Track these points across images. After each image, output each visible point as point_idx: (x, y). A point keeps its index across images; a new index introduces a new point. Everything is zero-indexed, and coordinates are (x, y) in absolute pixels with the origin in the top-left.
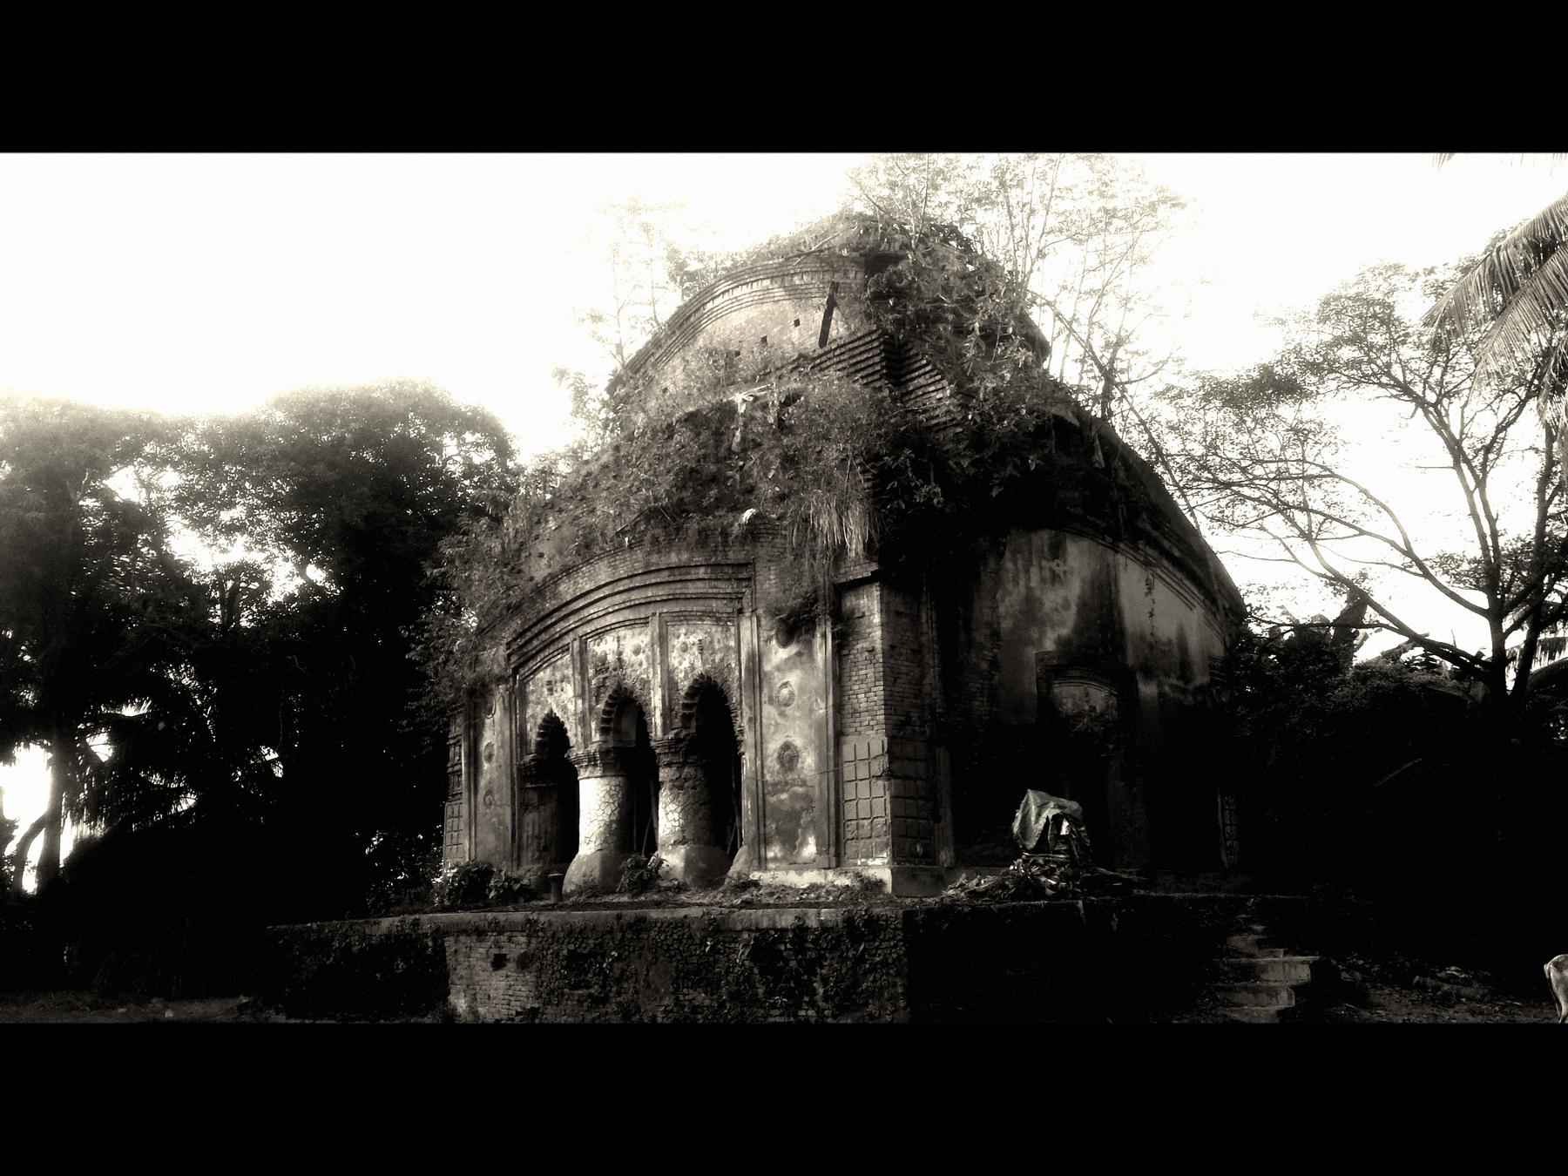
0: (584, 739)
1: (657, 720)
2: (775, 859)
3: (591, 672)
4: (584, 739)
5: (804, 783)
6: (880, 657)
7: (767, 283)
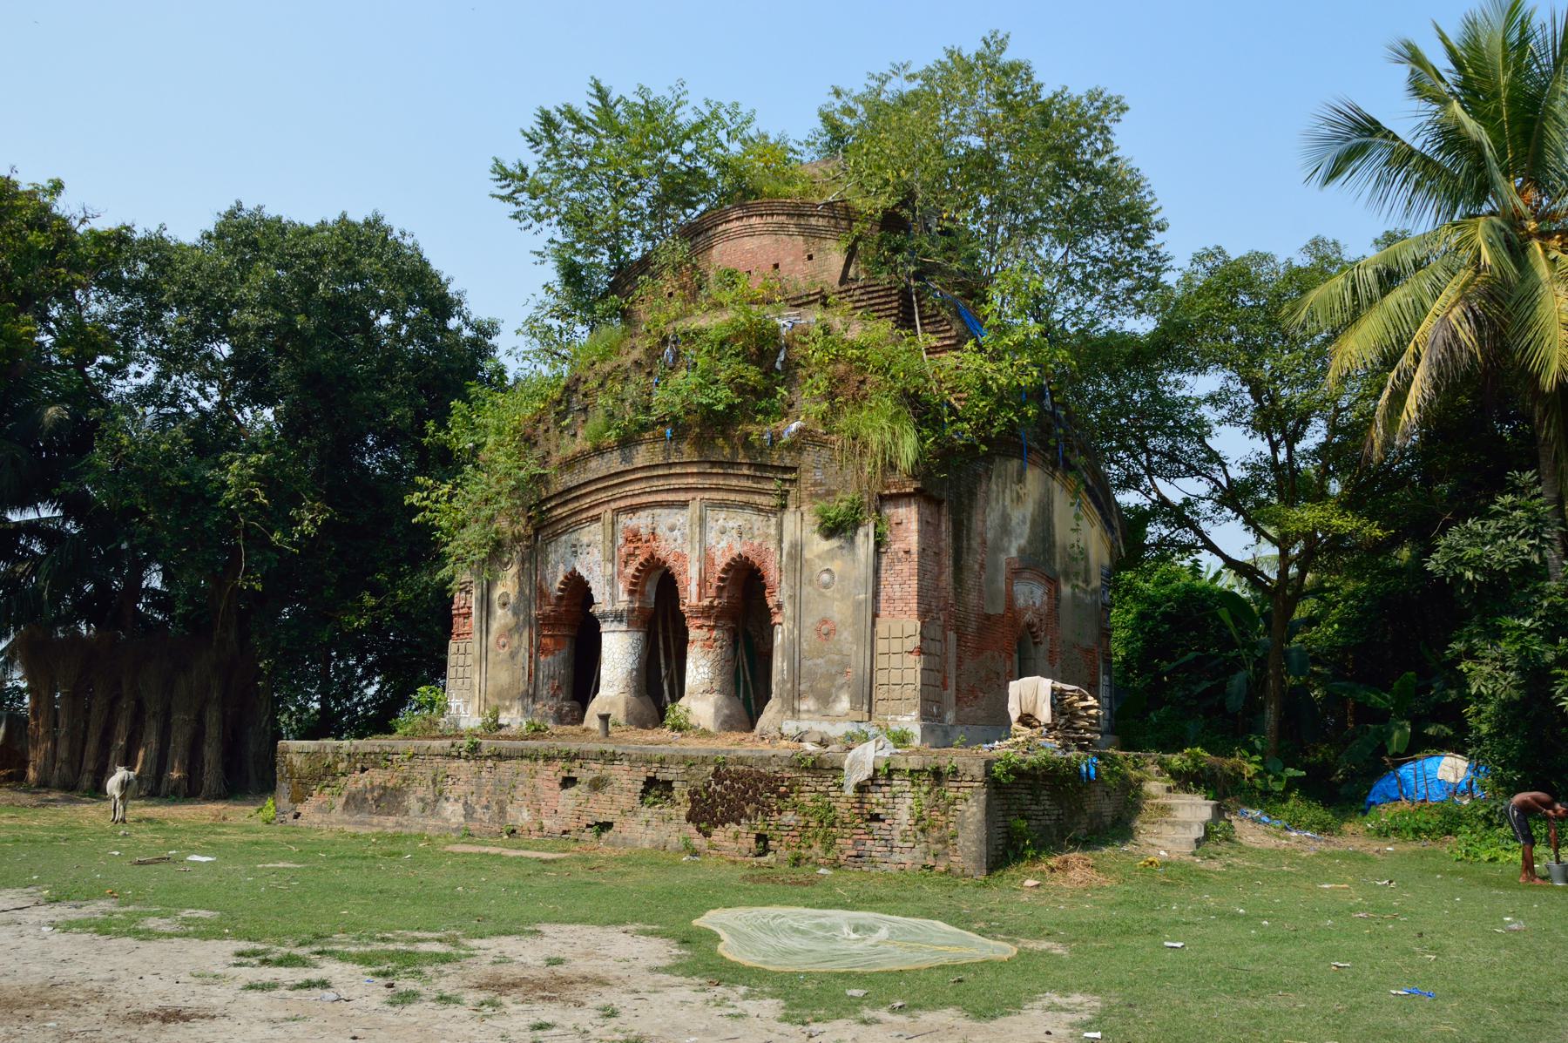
0: (610, 593)
1: (693, 588)
2: (808, 711)
3: (621, 541)
4: (610, 593)
5: (840, 652)
6: (915, 557)
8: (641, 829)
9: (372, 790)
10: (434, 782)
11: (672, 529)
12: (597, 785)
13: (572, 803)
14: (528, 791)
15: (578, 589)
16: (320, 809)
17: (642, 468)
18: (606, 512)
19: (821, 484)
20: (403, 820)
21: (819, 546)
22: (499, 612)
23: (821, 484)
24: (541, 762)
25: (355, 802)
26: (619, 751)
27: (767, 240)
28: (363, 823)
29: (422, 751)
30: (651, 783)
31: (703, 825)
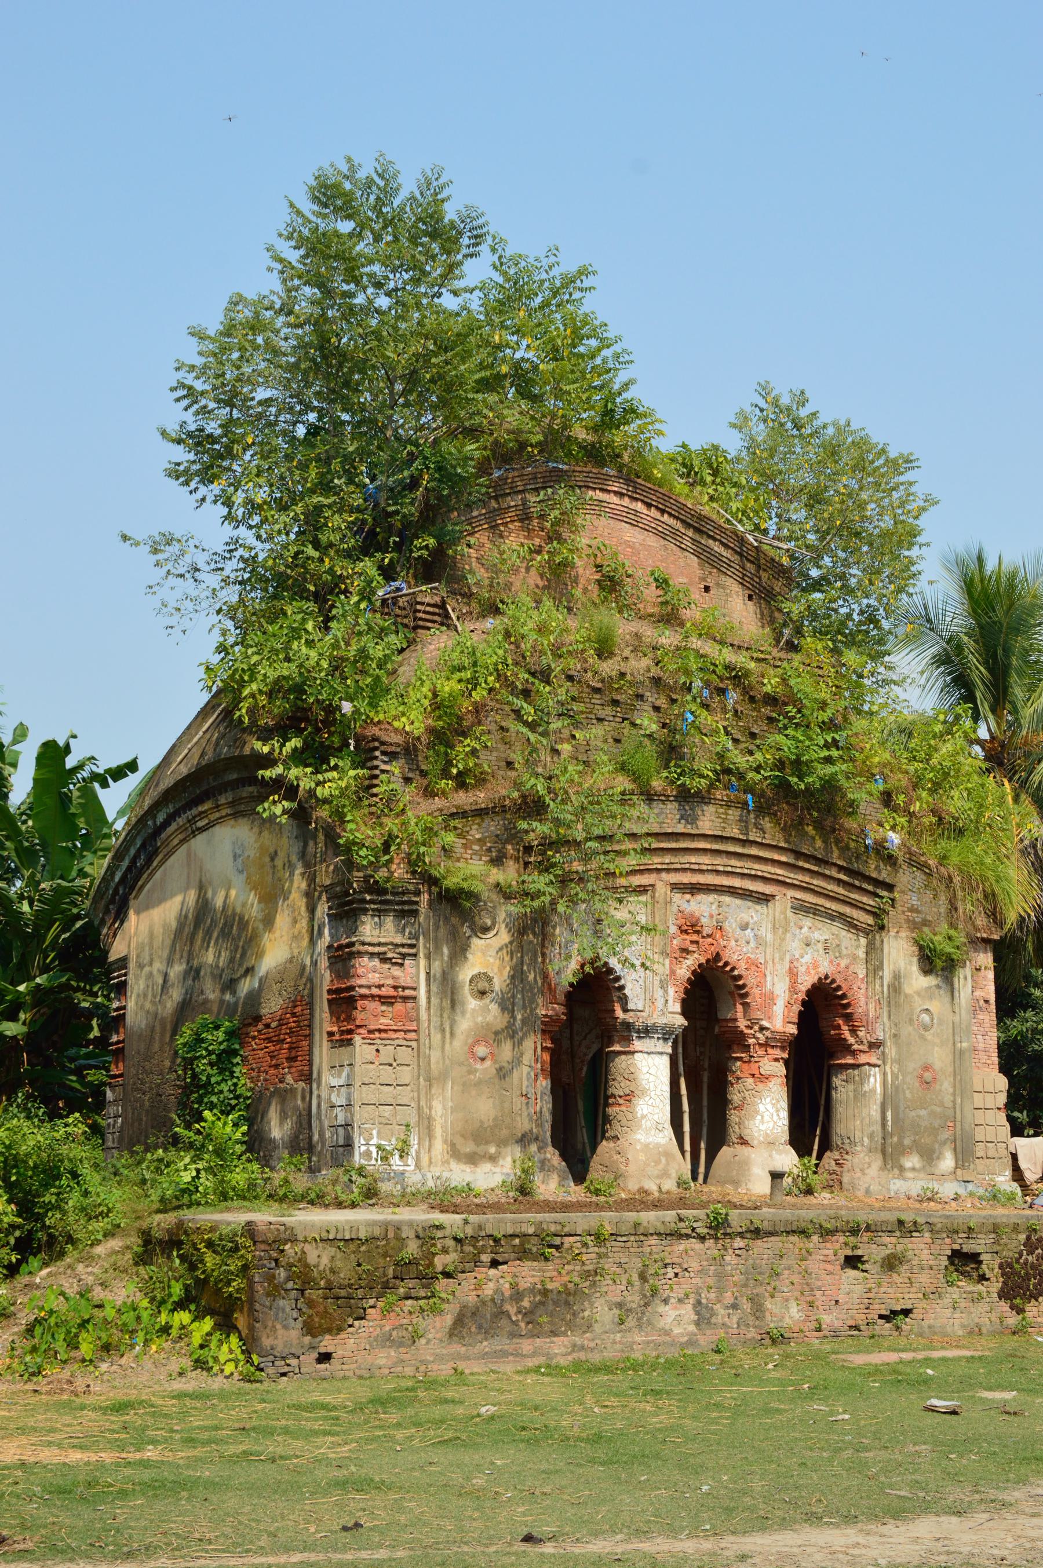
1: (779, 1009)
2: (913, 1169)
5: (942, 1104)
7: (672, 521)
8: (948, 1312)
9: (517, 1295)
10: (643, 1277)
11: (744, 927)
12: (891, 1264)
13: (859, 1289)
14: (796, 1278)
15: (596, 989)
17: (704, 837)
18: (662, 884)
19: (917, 911)
20: (585, 1340)
21: (918, 982)
23: (917, 911)
24: (815, 1238)
26: (921, 1220)
27: (652, 541)
29: (624, 1230)
30: (848, 1259)
31: (1018, 1301)
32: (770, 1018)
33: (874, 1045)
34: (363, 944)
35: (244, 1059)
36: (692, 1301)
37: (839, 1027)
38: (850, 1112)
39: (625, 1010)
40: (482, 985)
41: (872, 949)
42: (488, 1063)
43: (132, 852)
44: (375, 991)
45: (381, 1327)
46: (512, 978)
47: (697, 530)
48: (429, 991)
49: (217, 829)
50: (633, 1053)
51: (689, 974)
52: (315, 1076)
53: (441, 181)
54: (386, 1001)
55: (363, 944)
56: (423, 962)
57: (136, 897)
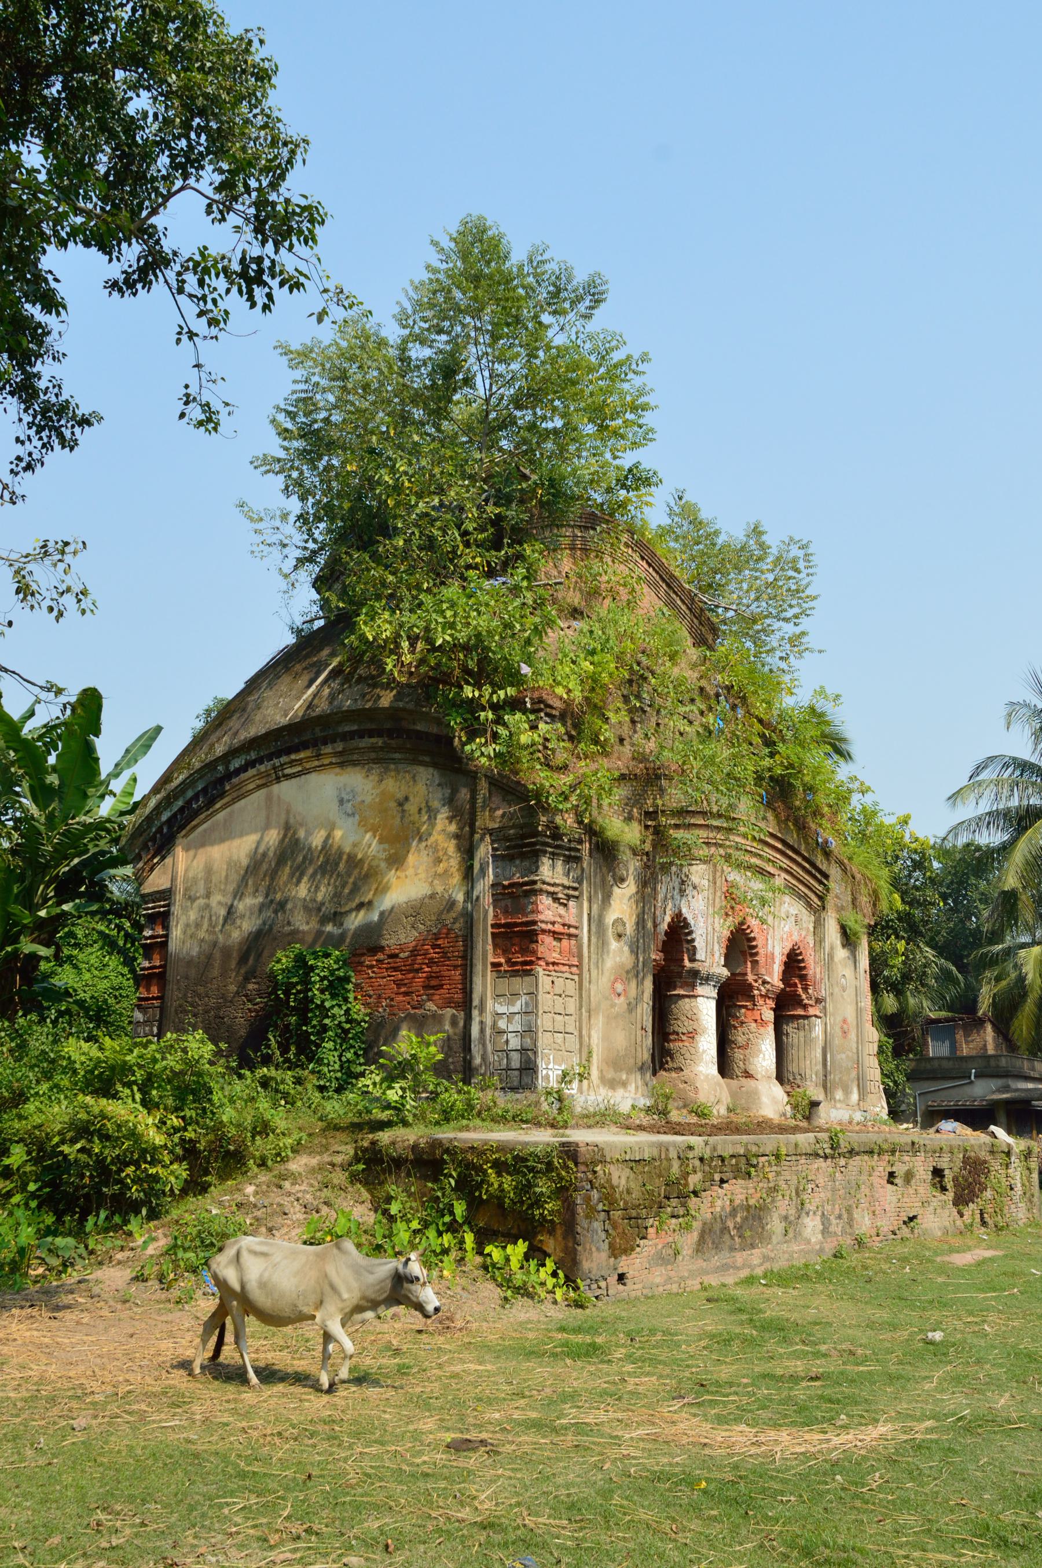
0: (709, 954)
9: (734, 1212)
16: (661, 1259)
22: (614, 945)
25: (712, 1237)
28: (725, 1268)
32: (771, 974)
33: (818, 1001)
34: (544, 883)
35: (357, 986)
36: (819, 1213)
37: (795, 985)
38: (801, 1054)
39: (692, 960)
40: (620, 929)
41: (819, 924)
42: (622, 998)
43: (190, 794)
44: (550, 927)
45: (656, 1245)
46: (637, 924)
47: (668, 585)
48: (589, 931)
49: (313, 777)
50: (695, 997)
51: (728, 934)
52: (476, 1002)
53: (545, 257)
54: (557, 936)
55: (544, 883)
56: (586, 905)
57: (186, 836)
